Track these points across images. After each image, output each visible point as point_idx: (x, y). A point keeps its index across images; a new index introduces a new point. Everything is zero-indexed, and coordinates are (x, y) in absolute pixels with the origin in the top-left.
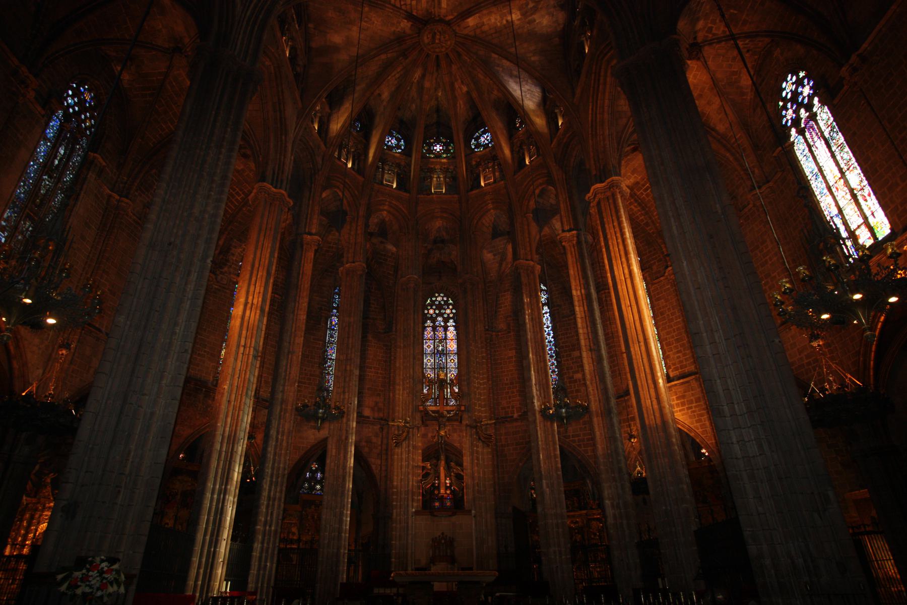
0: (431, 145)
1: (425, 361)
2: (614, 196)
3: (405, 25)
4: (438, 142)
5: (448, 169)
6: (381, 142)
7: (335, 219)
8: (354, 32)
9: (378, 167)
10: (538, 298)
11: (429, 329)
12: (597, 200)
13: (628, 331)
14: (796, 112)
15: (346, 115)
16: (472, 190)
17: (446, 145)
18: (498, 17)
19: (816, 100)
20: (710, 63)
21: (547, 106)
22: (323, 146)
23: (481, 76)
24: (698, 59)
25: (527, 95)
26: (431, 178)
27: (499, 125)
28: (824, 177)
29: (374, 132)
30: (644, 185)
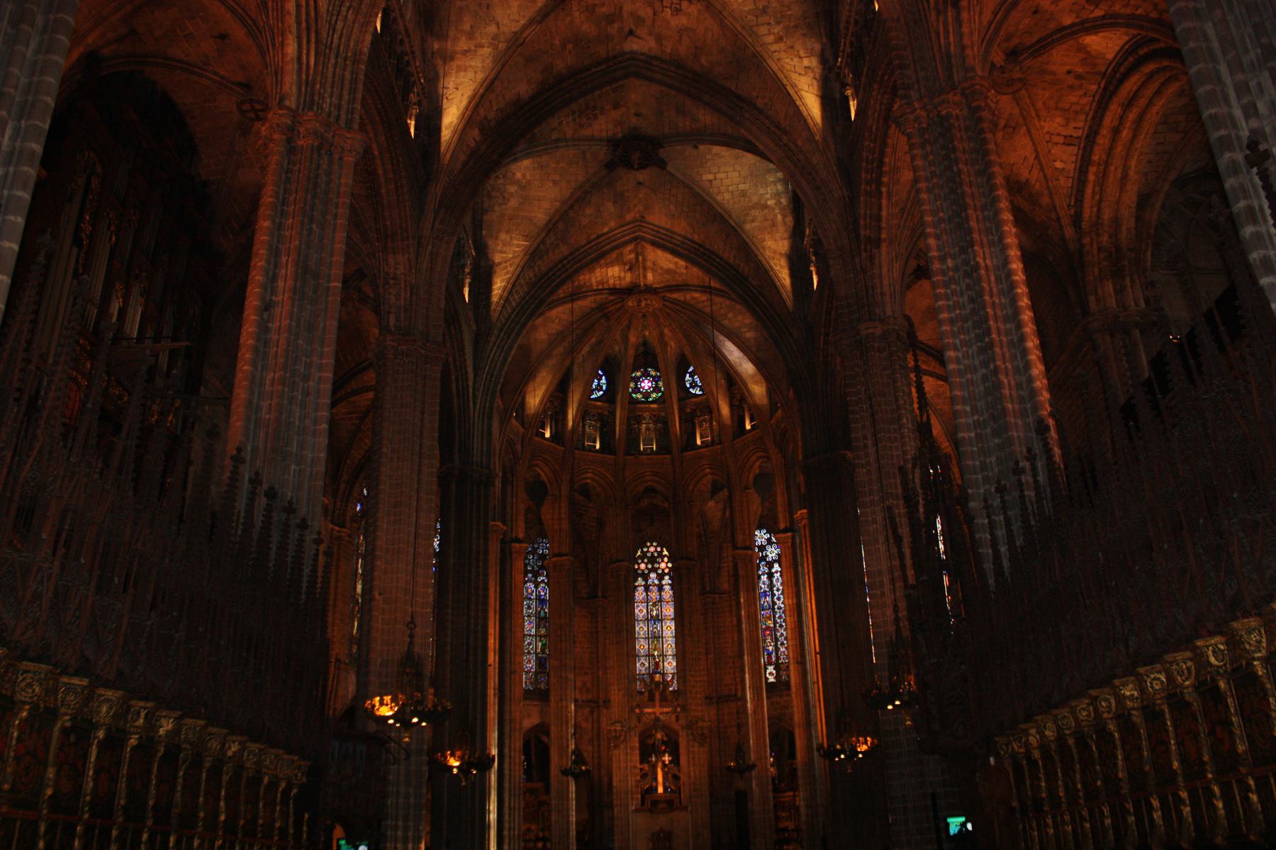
4: (646, 375)
11: (641, 589)
15: (544, 387)
17: (656, 379)
22: (522, 430)
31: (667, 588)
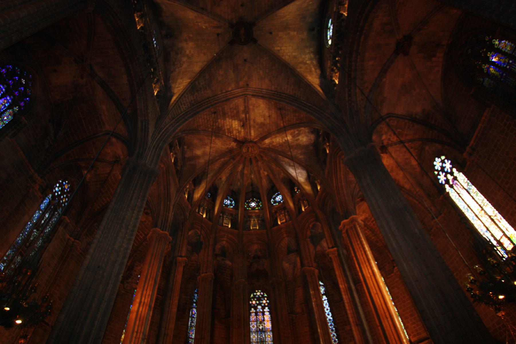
0: (249, 203)
1: (251, 337)
2: (355, 226)
3: (233, 144)
4: (253, 201)
5: (259, 215)
6: (222, 202)
7: (196, 247)
8: (207, 149)
9: (220, 216)
10: (319, 290)
11: (253, 314)
12: (345, 229)
13: (379, 311)
14: (445, 176)
16: (274, 226)
17: (258, 202)
18: (280, 139)
19: (454, 170)
20: (393, 154)
21: (310, 179)
22: (190, 207)
23: (274, 167)
24: (387, 153)
25: (299, 175)
26: (250, 221)
27: (286, 191)
28: (472, 210)
29: (218, 198)
30: (371, 219)
31: (267, 313)
